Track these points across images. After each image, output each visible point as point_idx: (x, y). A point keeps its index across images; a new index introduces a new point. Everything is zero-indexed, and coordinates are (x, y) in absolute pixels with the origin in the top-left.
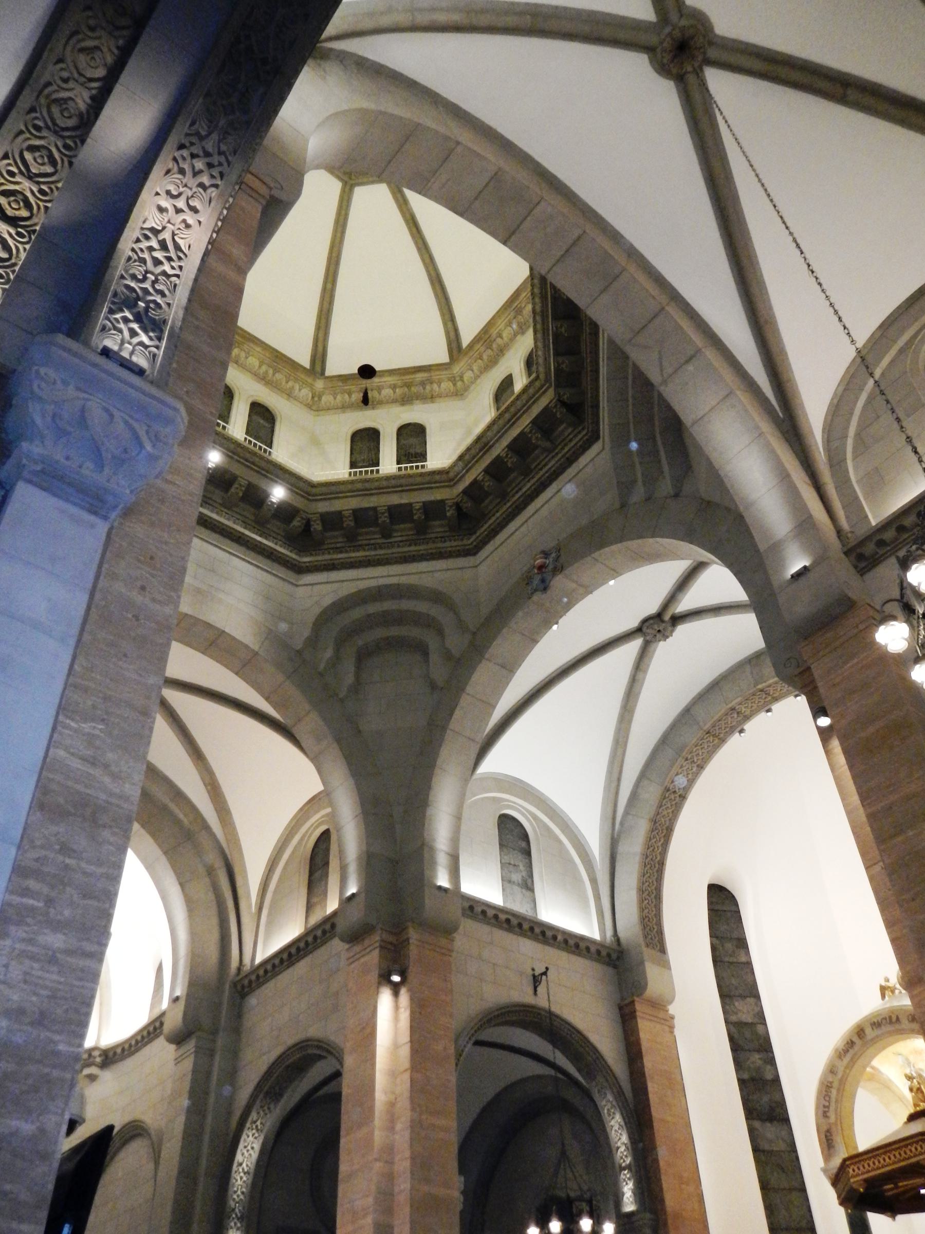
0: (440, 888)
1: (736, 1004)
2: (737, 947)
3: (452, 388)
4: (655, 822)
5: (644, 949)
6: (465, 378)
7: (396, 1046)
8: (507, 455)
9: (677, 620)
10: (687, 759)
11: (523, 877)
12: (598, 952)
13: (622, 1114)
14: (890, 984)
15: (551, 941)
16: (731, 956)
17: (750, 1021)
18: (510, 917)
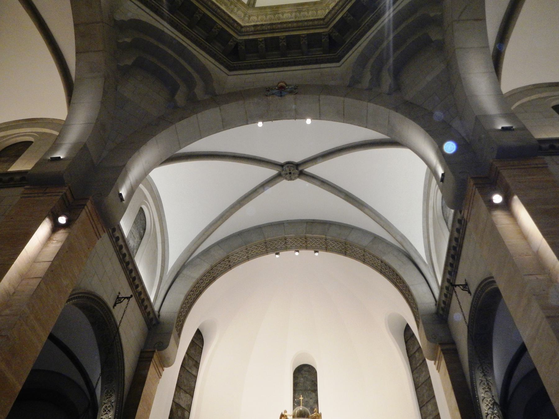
0: (121, 195)
1: (181, 393)
2: (194, 365)
3: (242, 16)
4: (212, 269)
5: (174, 327)
6: (251, 18)
7: (35, 260)
8: (283, 39)
9: (302, 174)
10: (246, 249)
11: (134, 246)
12: (149, 314)
13: (116, 412)
14: (286, 414)
15: (134, 287)
16: (190, 368)
17: (183, 406)
18: (127, 256)
